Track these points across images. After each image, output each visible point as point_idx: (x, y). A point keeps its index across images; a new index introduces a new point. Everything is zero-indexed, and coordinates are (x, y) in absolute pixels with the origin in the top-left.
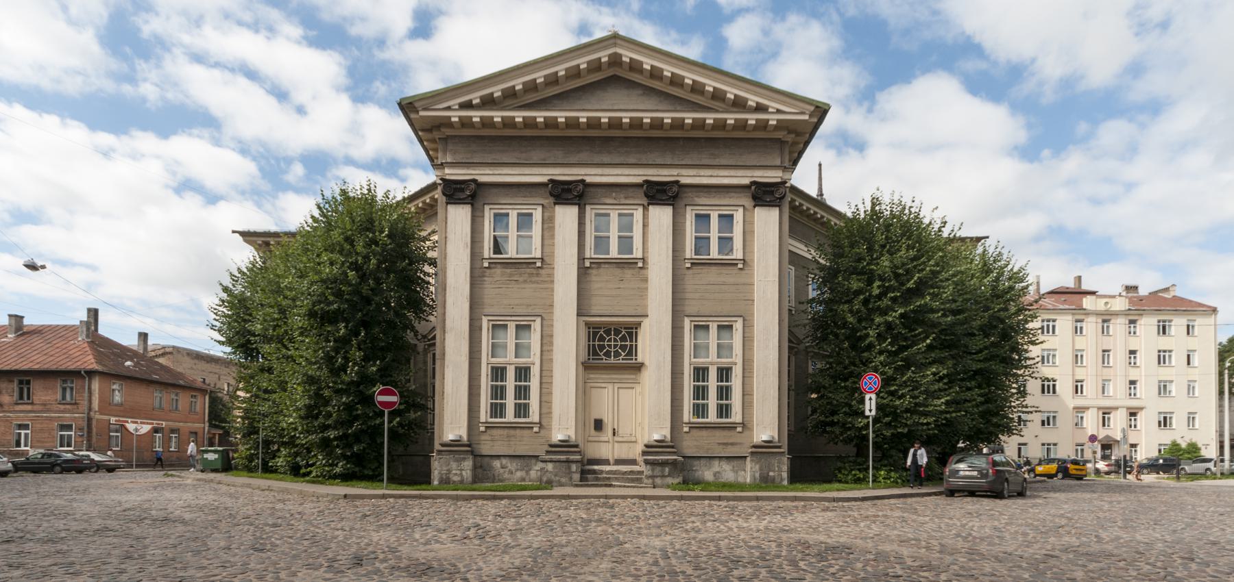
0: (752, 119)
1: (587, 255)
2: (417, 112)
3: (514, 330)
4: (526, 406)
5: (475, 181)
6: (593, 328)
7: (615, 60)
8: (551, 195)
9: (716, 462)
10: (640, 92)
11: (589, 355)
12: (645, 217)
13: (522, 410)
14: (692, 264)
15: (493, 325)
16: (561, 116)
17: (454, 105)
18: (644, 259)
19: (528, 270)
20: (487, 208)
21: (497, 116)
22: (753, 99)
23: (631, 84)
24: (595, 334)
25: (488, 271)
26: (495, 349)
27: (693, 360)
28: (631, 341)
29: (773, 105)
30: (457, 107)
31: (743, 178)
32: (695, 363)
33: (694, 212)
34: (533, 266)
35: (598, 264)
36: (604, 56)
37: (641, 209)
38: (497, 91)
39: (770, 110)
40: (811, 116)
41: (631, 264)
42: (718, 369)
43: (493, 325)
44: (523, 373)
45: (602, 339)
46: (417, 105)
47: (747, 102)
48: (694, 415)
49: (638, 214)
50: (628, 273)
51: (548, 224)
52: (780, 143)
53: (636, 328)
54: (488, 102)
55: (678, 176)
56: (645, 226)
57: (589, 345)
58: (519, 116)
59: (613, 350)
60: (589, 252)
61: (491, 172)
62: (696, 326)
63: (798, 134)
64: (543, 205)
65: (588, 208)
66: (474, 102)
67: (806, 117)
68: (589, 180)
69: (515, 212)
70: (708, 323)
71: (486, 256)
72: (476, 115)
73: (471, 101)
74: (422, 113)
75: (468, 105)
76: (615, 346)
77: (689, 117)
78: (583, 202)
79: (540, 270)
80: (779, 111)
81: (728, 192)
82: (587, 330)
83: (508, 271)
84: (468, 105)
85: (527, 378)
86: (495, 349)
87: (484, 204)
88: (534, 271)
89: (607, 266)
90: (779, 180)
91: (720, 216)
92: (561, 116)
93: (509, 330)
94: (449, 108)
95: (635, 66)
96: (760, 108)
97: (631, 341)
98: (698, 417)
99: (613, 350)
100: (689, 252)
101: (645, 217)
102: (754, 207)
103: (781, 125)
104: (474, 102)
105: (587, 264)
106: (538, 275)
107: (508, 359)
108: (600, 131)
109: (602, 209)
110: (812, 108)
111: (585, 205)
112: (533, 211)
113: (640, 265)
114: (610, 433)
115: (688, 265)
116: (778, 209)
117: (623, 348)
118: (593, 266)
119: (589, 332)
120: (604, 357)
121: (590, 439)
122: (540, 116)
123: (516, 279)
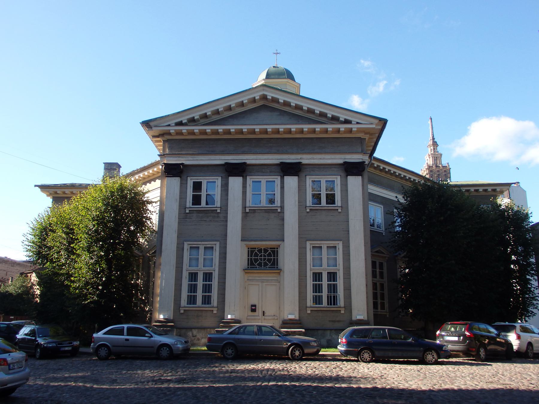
0: (343, 127)
1: (248, 205)
3: (203, 250)
4: (210, 297)
5: (182, 164)
6: (251, 248)
7: (264, 97)
8: (226, 171)
9: (328, 332)
10: (278, 113)
11: (248, 265)
13: (207, 300)
14: (310, 209)
15: (190, 247)
16: (233, 128)
17: (172, 124)
18: (282, 207)
19: (212, 214)
20: (189, 178)
21: (196, 129)
22: (342, 118)
23: (273, 110)
24: (252, 252)
25: (188, 215)
26: (194, 261)
27: (312, 268)
28: (274, 256)
29: (354, 120)
30: (174, 125)
31: (339, 159)
32: (313, 269)
33: (311, 180)
34: (215, 212)
35: (253, 211)
37: (279, 178)
39: (353, 123)
41: (274, 211)
42: (328, 273)
43: (190, 247)
44: (208, 276)
45: (256, 255)
46: (152, 124)
47: (339, 119)
48: (313, 302)
49: (278, 179)
50: (272, 215)
51: (225, 187)
52: (361, 140)
53: (277, 248)
54: (192, 121)
55: (301, 159)
56: (282, 187)
57: (248, 259)
58: (209, 129)
59: (263, 262)
61: (192, 159)
62: (313, 247)
63: (371, 134)
64: (221, 176)
65: (248, 178)
66: (183, 122)
67: (374, 126)
68: (248, 162)
69: (206, 181)
70: (321, 245)
71: (188, 206)
72: (184, 129)
73: (182, 121)
75: (180, 124)
76: (264, 259)
77: (306, 127)
78: (244, 175)
79: (219, 214)
80: (358, 123)
81: (331, 168)
82: (247, 250)
83: (201, 215)
84: (180, 124)
85: (210, 280)
86: (194, 261)
87: (188, 177)
88: (216, 215)
89: (259, 211)
90: (361, 161)
91: (326, 181)
92: (233, 128)
93: (200, 250)
94: (169, 125)
95: (275, 100)
96: (347, 122)
97: (274, 256)
98: (316, 304)
99: (263, 262)
100: (309, 201)
102: (347, 176)
103: (359, 131)
105: (247, 211)
106: (218, 217)
107: (199, 268)
108: (255, 135)
109: (256, 178)
111: (246, 176)
112: (216, 180)
113: (279, 210)
114: (261, 314)
115: (308, 210)
116: (361, 176)
117: (269, 260)
118: (251, 211)
119: (248, 251)
120: (257, 266)
121: (248, 318)
122: (221, 128)
123: (205, 219)
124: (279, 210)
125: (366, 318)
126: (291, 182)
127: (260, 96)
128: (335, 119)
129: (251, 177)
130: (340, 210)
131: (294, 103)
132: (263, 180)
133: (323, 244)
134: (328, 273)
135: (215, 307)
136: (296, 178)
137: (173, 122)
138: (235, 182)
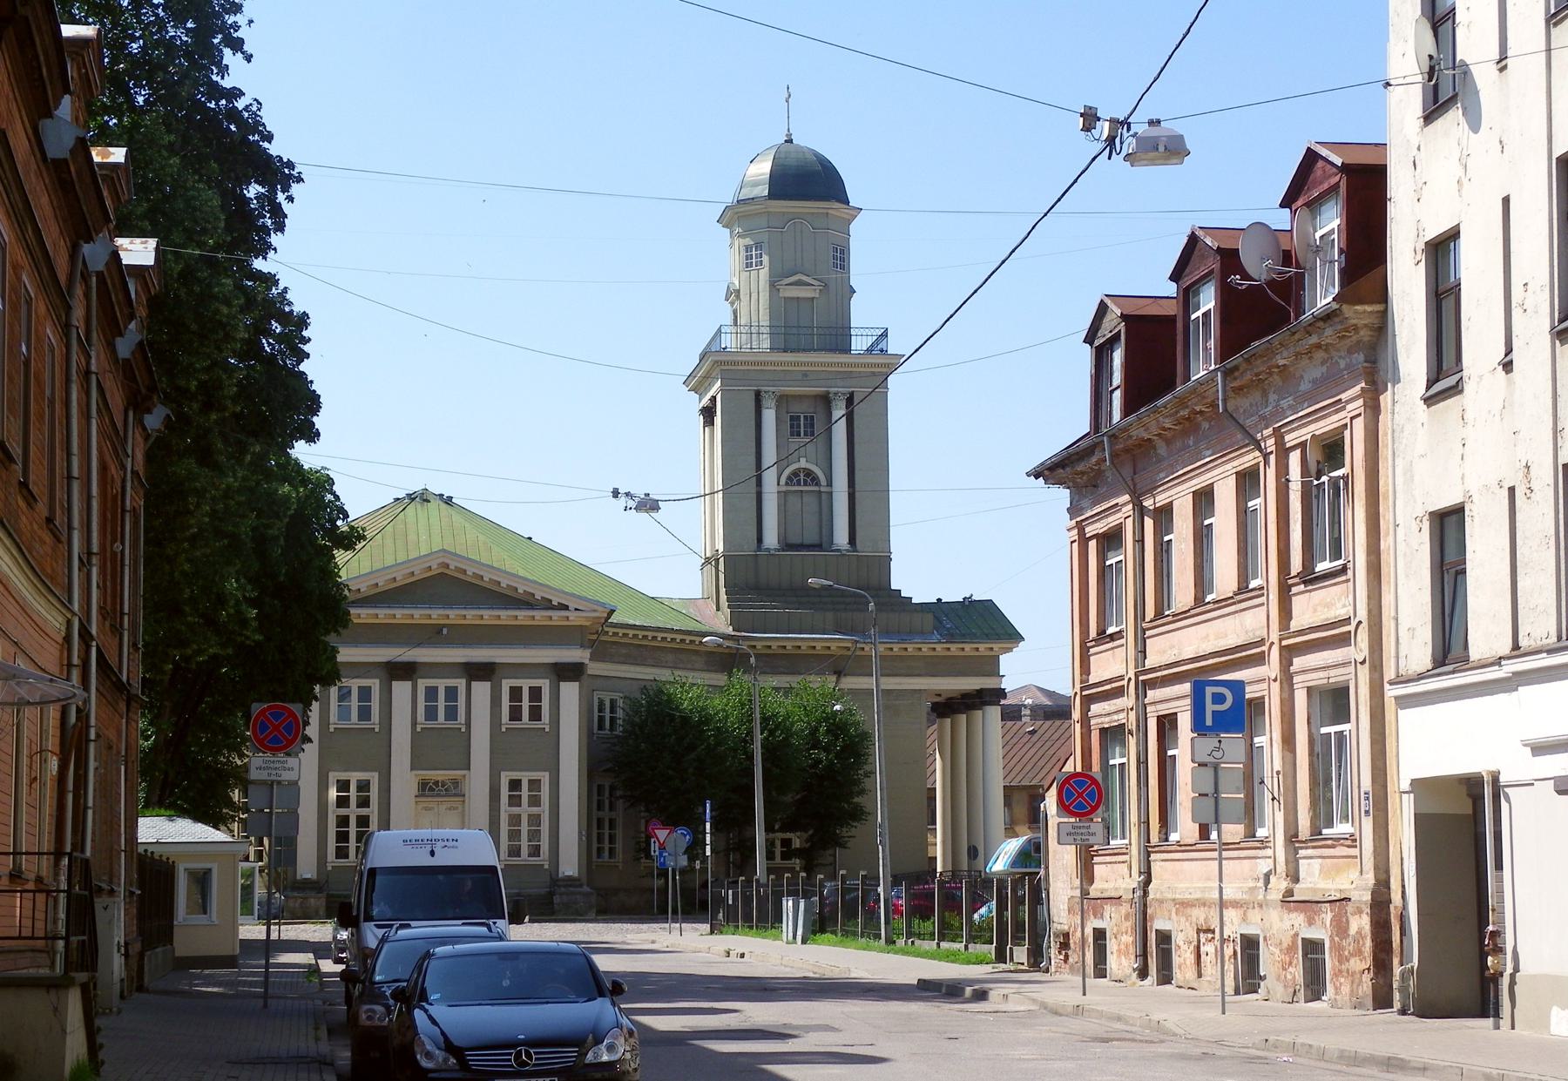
18: (468, 724)
65: (419, 680)
105: (419, 730)
124: (463, 730)
125: (576, 875)
126: (482, 689)
128: (547, 605)
132: (442, 684)
133: (523, 776)
136: (488, 684)
138: (401, 689)
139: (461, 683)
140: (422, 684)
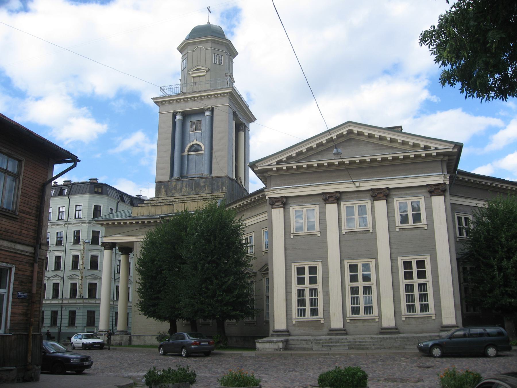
1: (343, 228)
2: (257, 167)
7: (350, 132)
12: (373, 207)
29: (433, 146)
30: (275, 164)
34: (316, 235)
36: (344, 131)
38: (293, 153)
39: (433, 148)
40: (453, 149)
49: (368, 204)
54: (289, 159)
60: (344, 226)
66: (283, 160)
67: (451, 150)
73: (282, 160)
74: (259, 168)
75: (280, 162)
96: (426, 148)
101: (373, 207)
103: (438, 154)
104: (283, 160)
110: (453, 145)
113: (371, 231)
116: (443, 196)
126: (381, 205)
127: (347, 131)
129: (345, 203)
130: (426, 228)
131: (377, 135)
134: (419, 284)
135: (322, 318)
137: (274, 162)
139: (368, 204)
140: (344, 205)
